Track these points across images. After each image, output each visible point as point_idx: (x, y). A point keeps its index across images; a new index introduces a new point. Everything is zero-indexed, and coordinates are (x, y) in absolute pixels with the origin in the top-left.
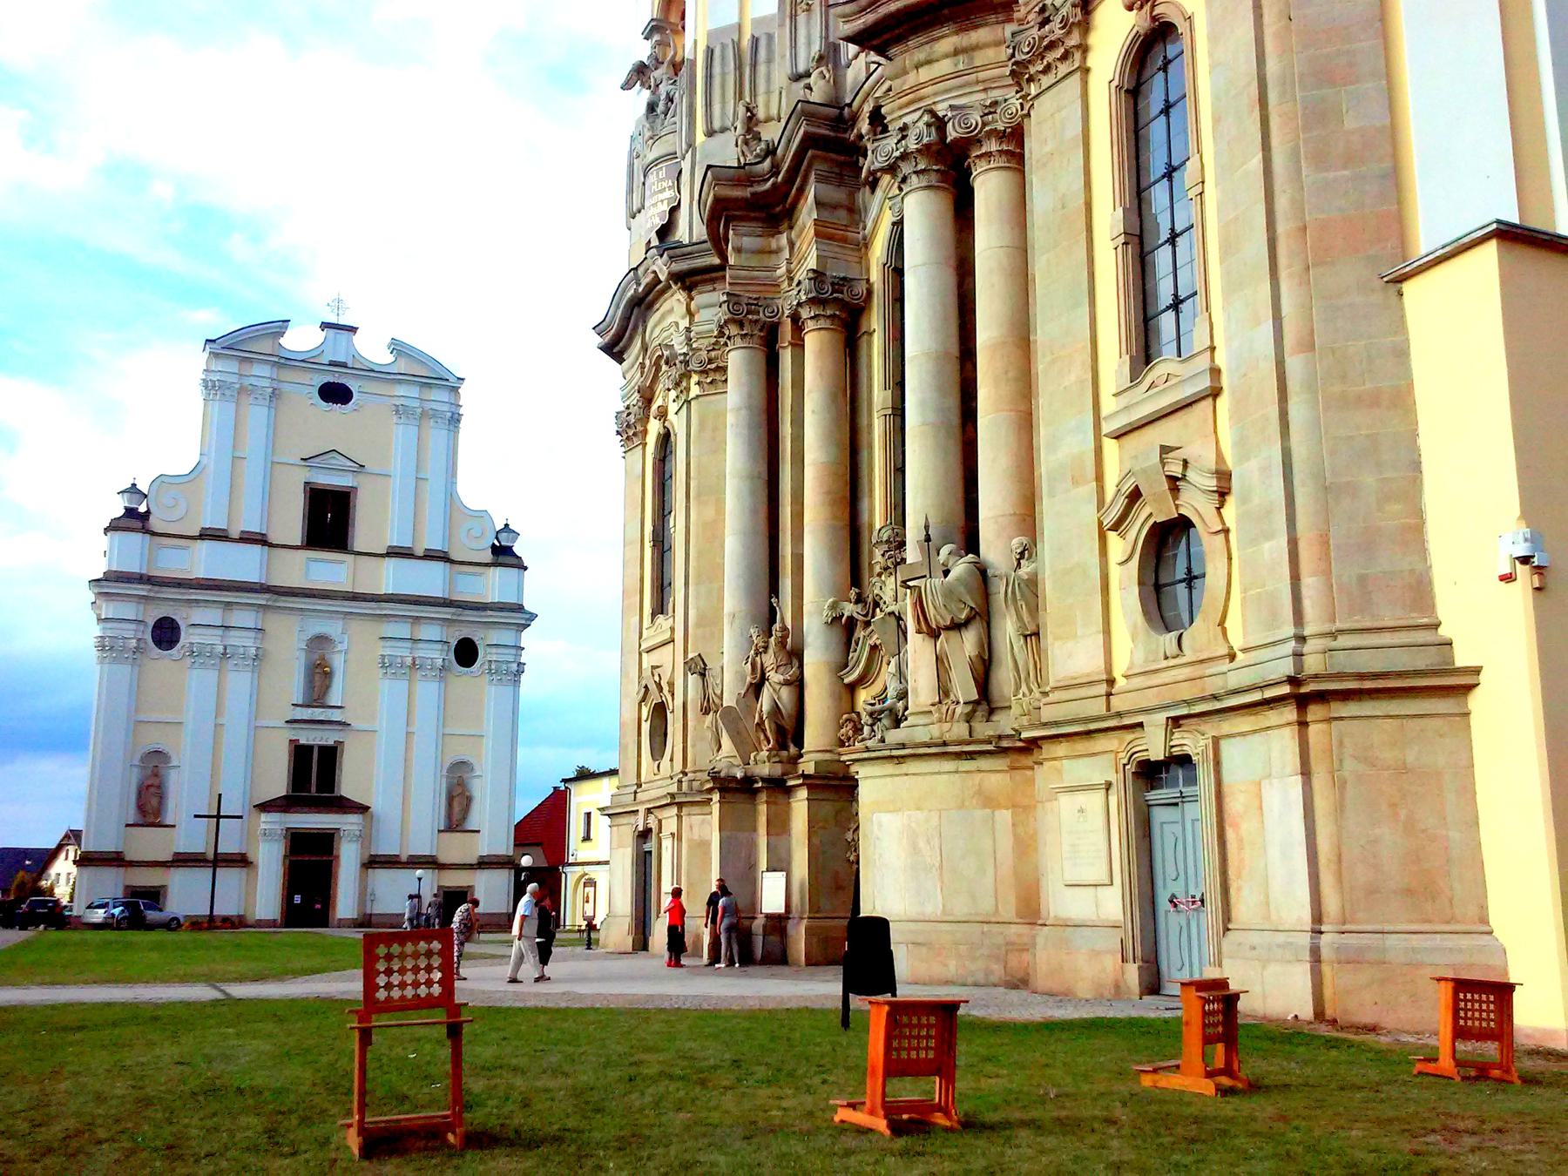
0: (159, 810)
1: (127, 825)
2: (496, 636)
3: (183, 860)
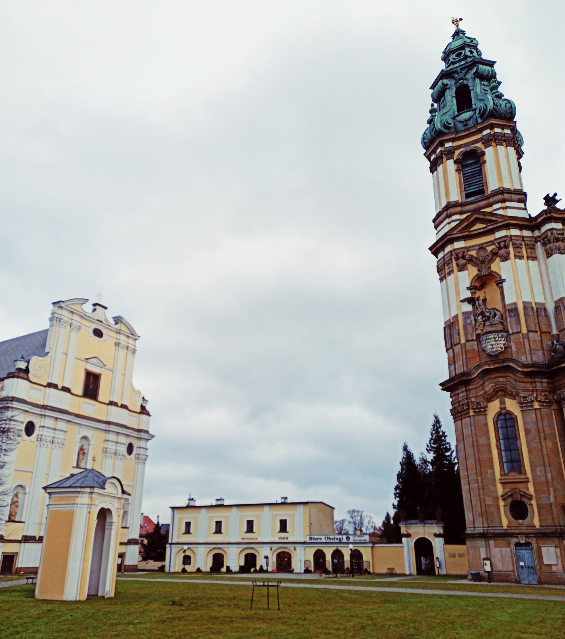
2: (142, 444)
3: (27, 539)
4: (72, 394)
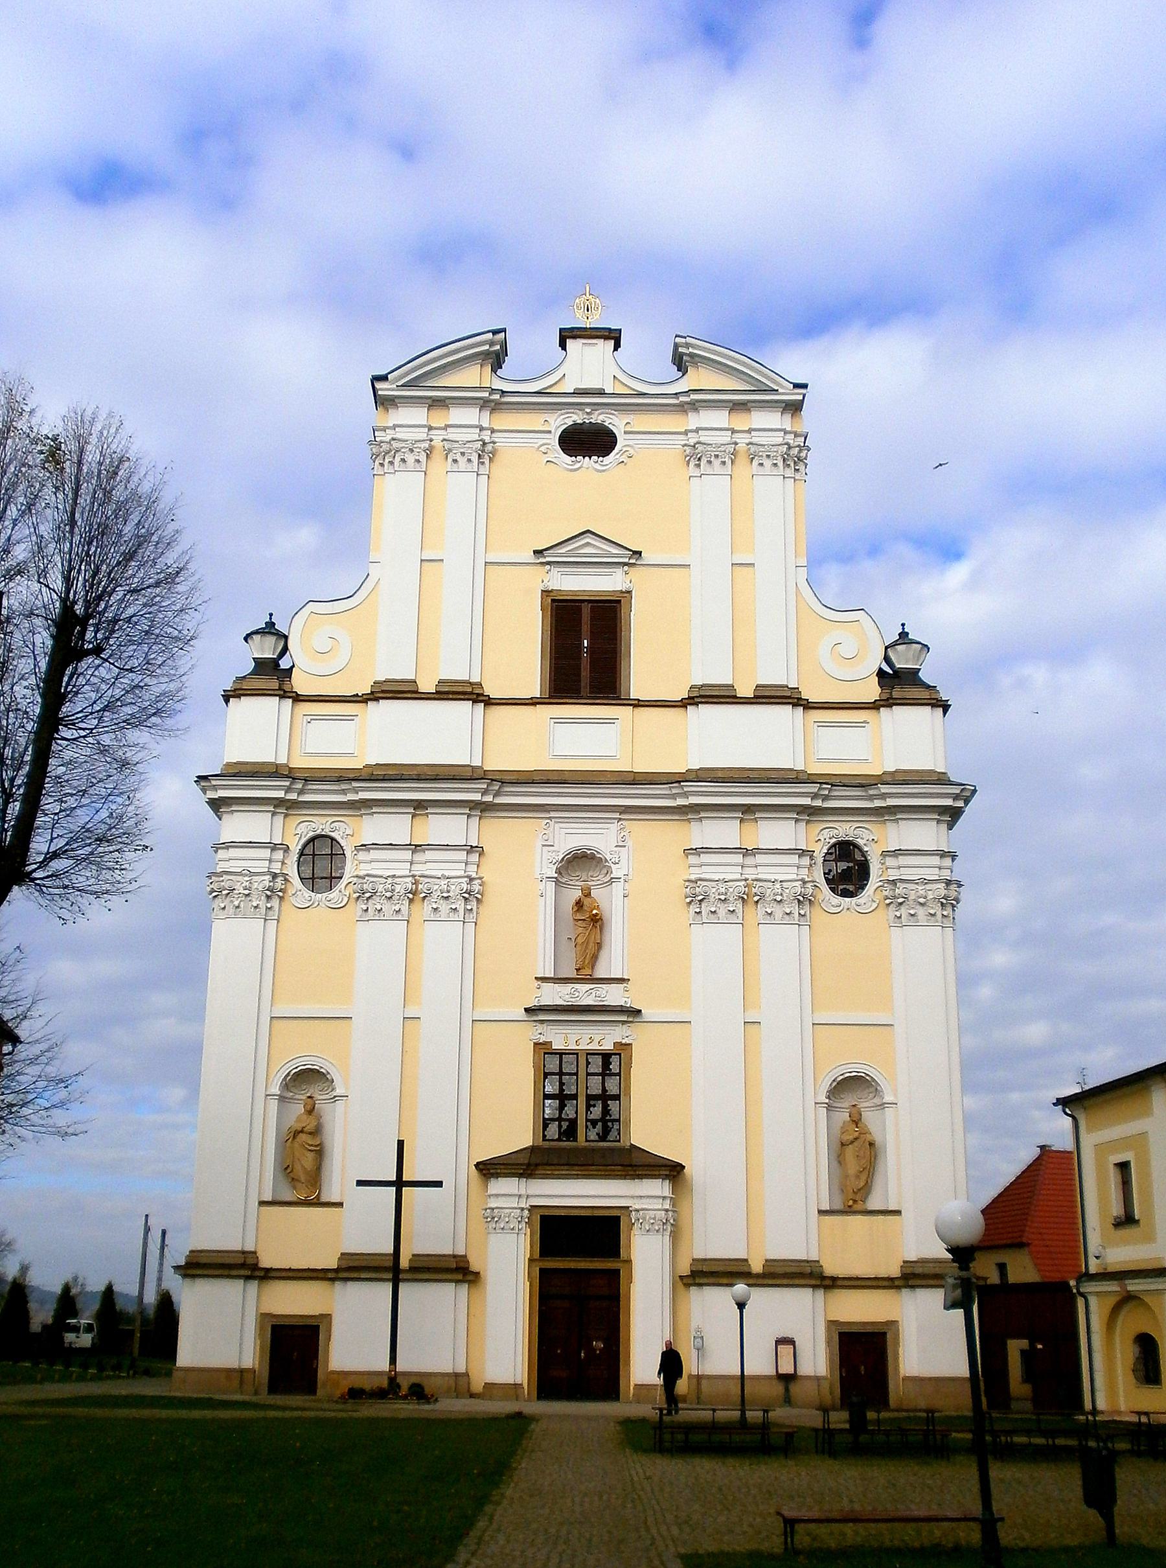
0: (315, 1177)
1: (262, 1203)
4: (489, 702)
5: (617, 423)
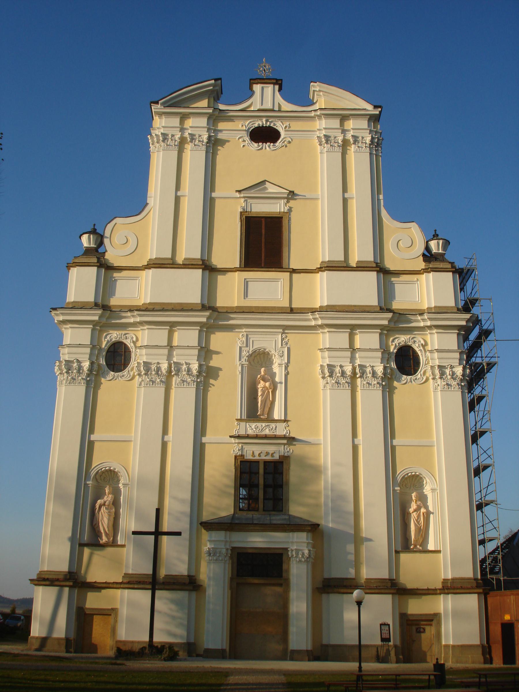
5: (279, 126)
